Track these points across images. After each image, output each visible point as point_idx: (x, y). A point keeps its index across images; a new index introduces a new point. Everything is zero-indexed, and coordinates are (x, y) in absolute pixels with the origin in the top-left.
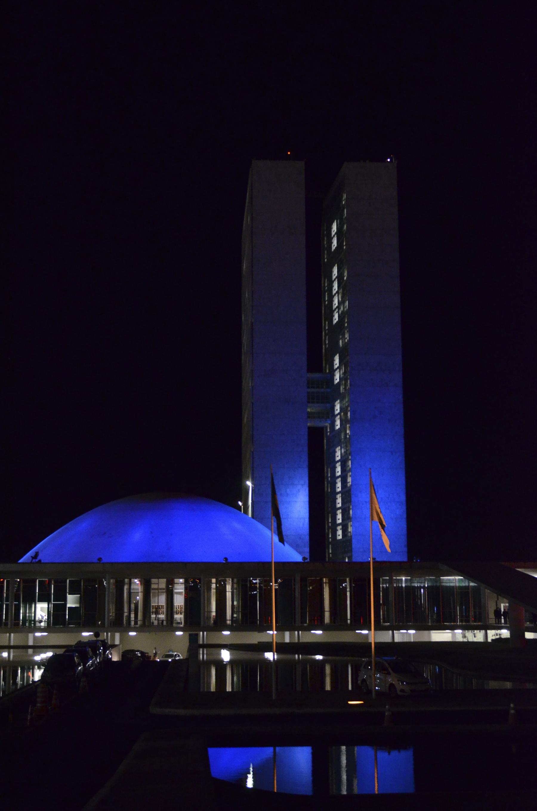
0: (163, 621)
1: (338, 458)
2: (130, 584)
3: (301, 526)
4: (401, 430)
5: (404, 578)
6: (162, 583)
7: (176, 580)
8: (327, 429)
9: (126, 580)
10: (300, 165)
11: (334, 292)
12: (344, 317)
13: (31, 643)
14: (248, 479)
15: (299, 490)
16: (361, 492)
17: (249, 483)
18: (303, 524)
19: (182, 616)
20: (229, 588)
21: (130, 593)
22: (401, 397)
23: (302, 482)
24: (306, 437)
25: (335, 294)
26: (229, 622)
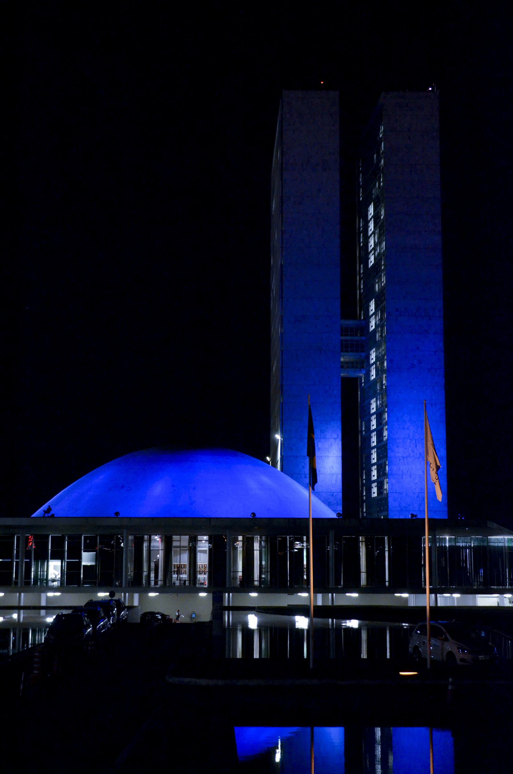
0: (185, 581)
1: (373, 411)
2: (150, 541)
3: (334, 482)
5: (447, 538)
6: (185, 540)
7: (200, 538)
8: (361, 381)
9: (146, 537)
11: (370, 233)
12: (381, 260)
13: (43, 603)
14: (276, 432)
15: (331, 444)
16: (398, 447)
17: (278, 437)
18: (336, 481)
19: (206, 576)
20: (256, 546)
21: (149, 551)
22: (442, 344)
23: (335, 436)
24: (339, 388)
25: (371, 235)
26: (256, 583)
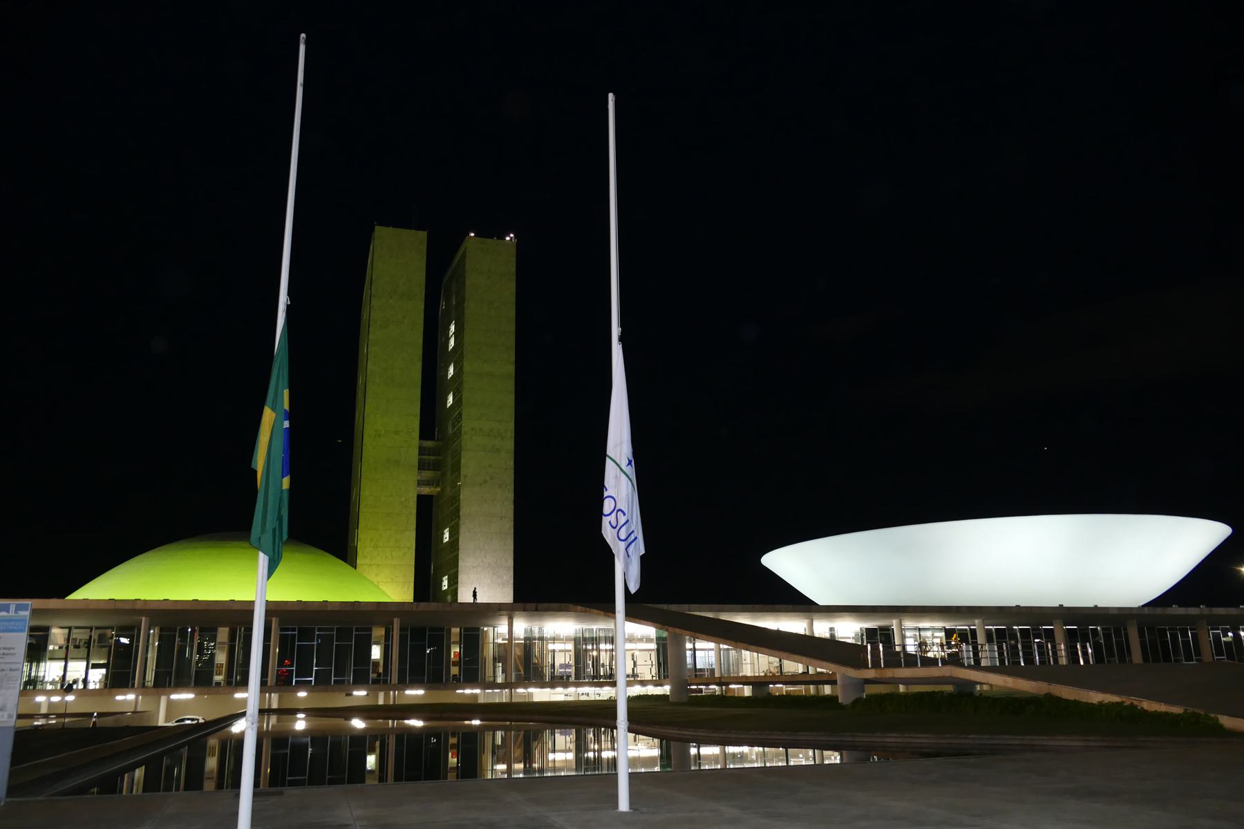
4: (511, 496)
22: (512, 463)
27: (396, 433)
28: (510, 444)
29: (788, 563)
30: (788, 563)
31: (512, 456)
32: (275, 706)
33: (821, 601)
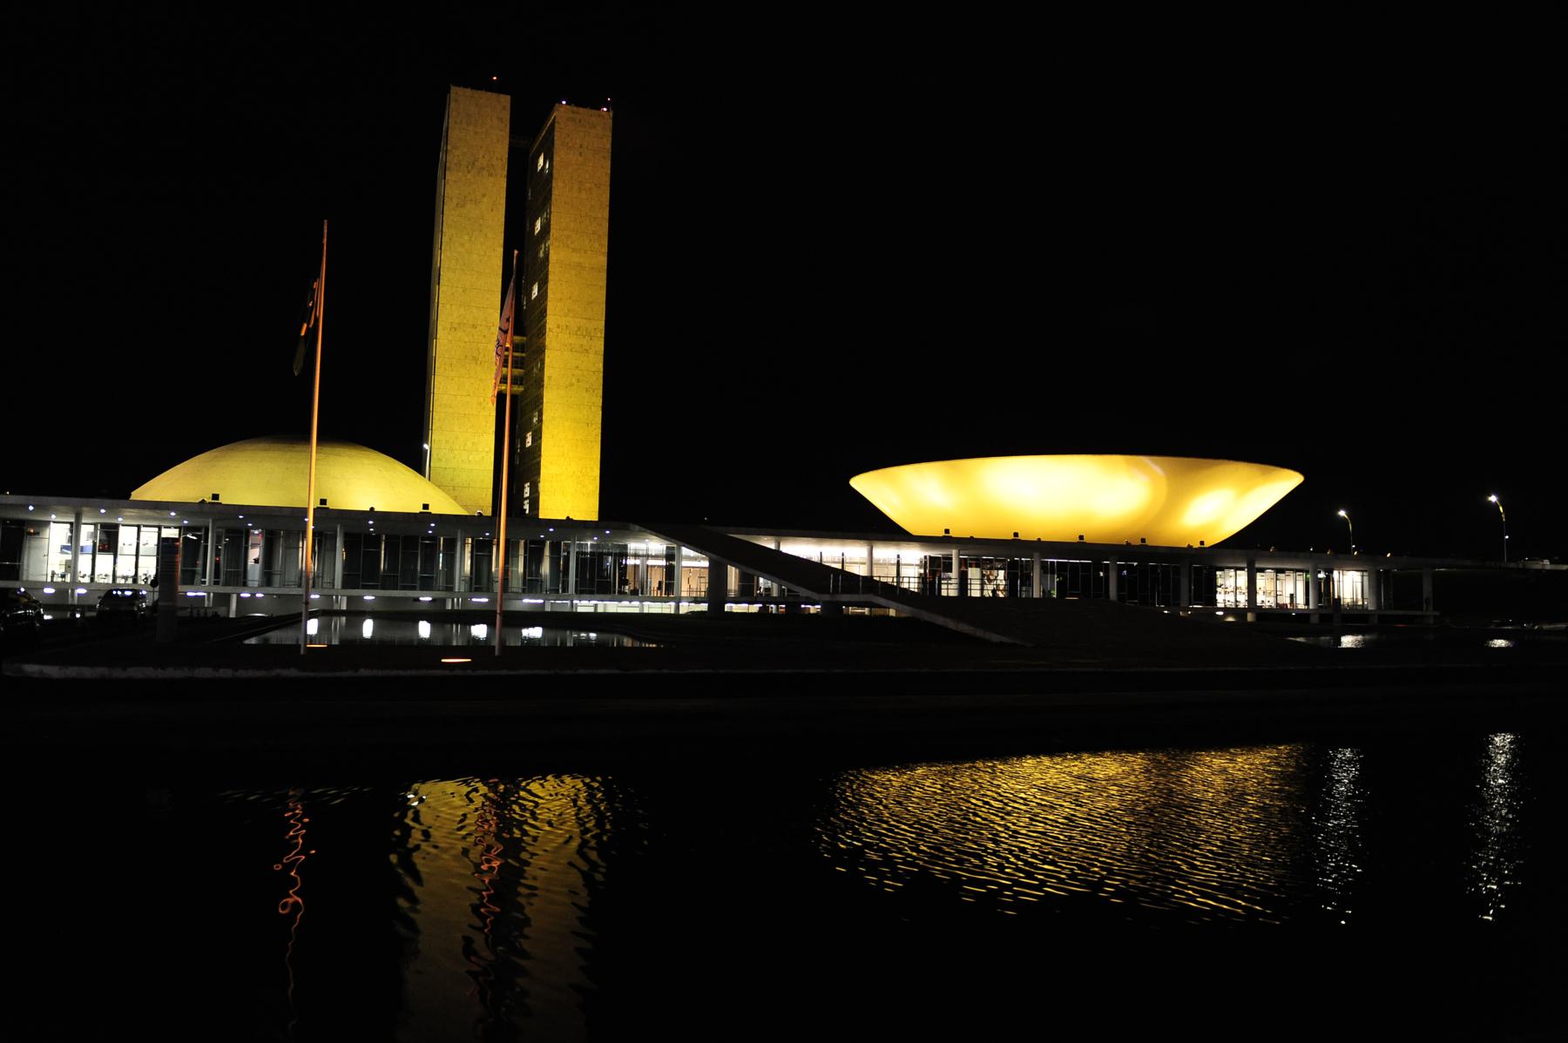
4: (599, 402)
10: (506, 100)
27: (474, 327)
28: (600, 345)
29: (880, 488)
30: (880, 488)
31: (601, 358)
32: (344, 607)
33: (914, 531)
